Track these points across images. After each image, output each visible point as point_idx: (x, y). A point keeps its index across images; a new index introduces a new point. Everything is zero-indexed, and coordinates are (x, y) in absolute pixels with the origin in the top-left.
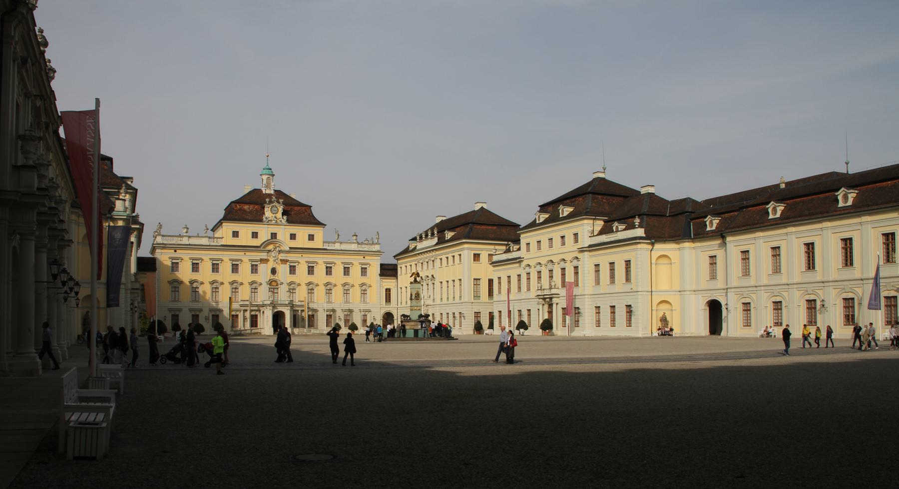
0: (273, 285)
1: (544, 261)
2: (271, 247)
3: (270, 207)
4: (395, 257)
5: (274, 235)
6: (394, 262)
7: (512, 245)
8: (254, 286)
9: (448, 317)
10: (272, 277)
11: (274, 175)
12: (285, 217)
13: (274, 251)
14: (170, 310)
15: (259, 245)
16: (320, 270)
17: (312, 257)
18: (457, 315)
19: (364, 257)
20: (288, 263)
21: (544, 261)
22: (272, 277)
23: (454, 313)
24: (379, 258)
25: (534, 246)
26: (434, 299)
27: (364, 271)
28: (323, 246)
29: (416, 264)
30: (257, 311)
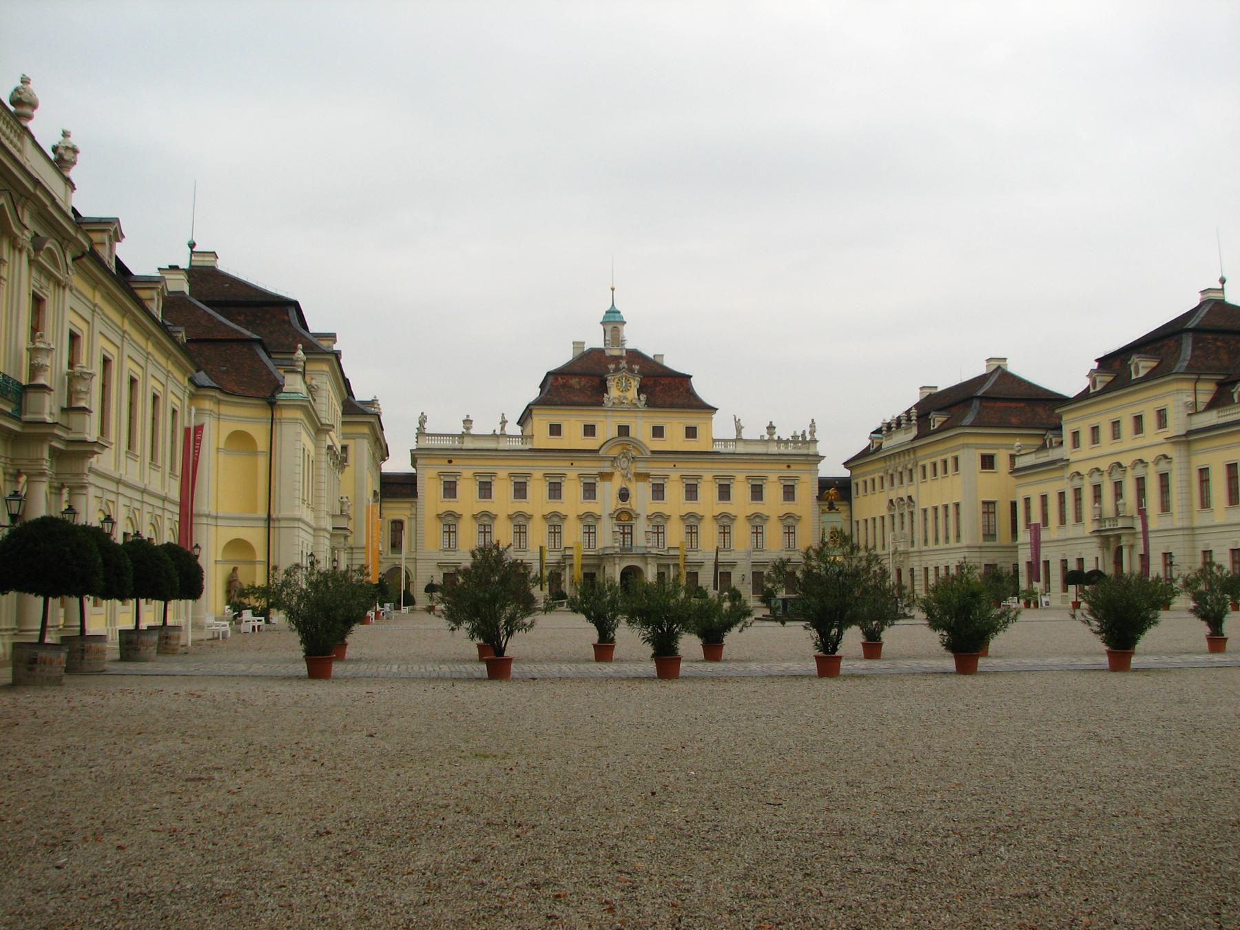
0: (625, 519)
1: (1104, 465)
3: (616, 380)
4: (844, 464)
5: (624, 430)
6: (846, 473)
7: (1050, 435)
8: (589, 522)
10: (621, 505)
11: (625, 323)
12: (643, 397)
14: (440, 565)
15: (597, 448)
16: (708, 491)
17: (690, 468)
19: (789, 466)
21: (1104, 465)
22: (621, 505)
25: (1085, 437)
27: (789, 493)
29: (882, 478)
30: (593, 565)
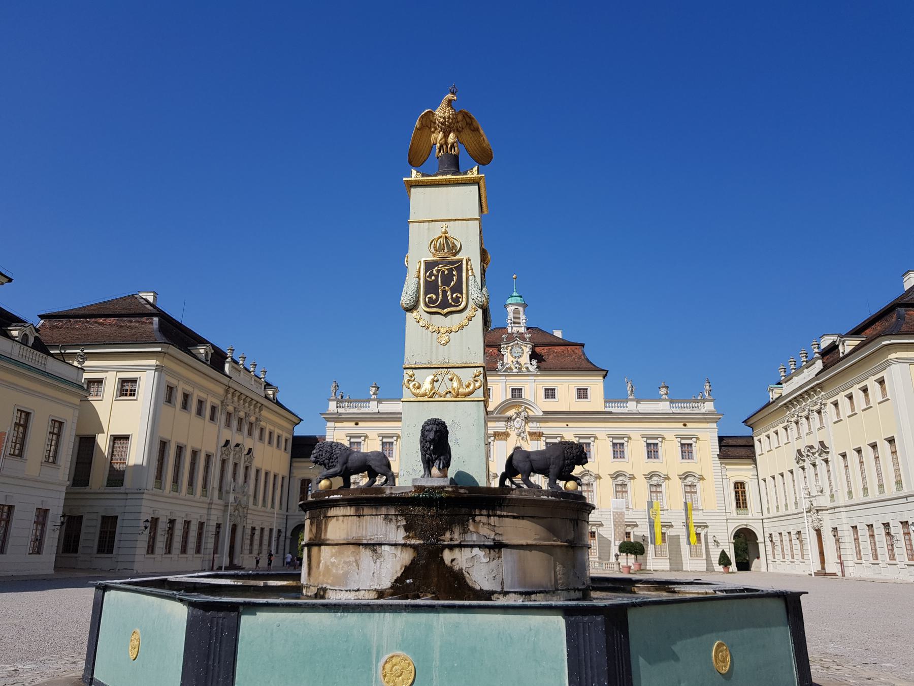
2: (511, 413)
3: (510, 348)
4: (743, 422)
5: (517, 392)
9: (872, 536)
12: (534, 362)
13: (516, 418)
18: (897, 530)
19: (685, 425)
20: (543, 439)
23: (886, 525)
24: (714, 425)
26: (832, 496)
27: (686, 450)
28: (606, 407)
